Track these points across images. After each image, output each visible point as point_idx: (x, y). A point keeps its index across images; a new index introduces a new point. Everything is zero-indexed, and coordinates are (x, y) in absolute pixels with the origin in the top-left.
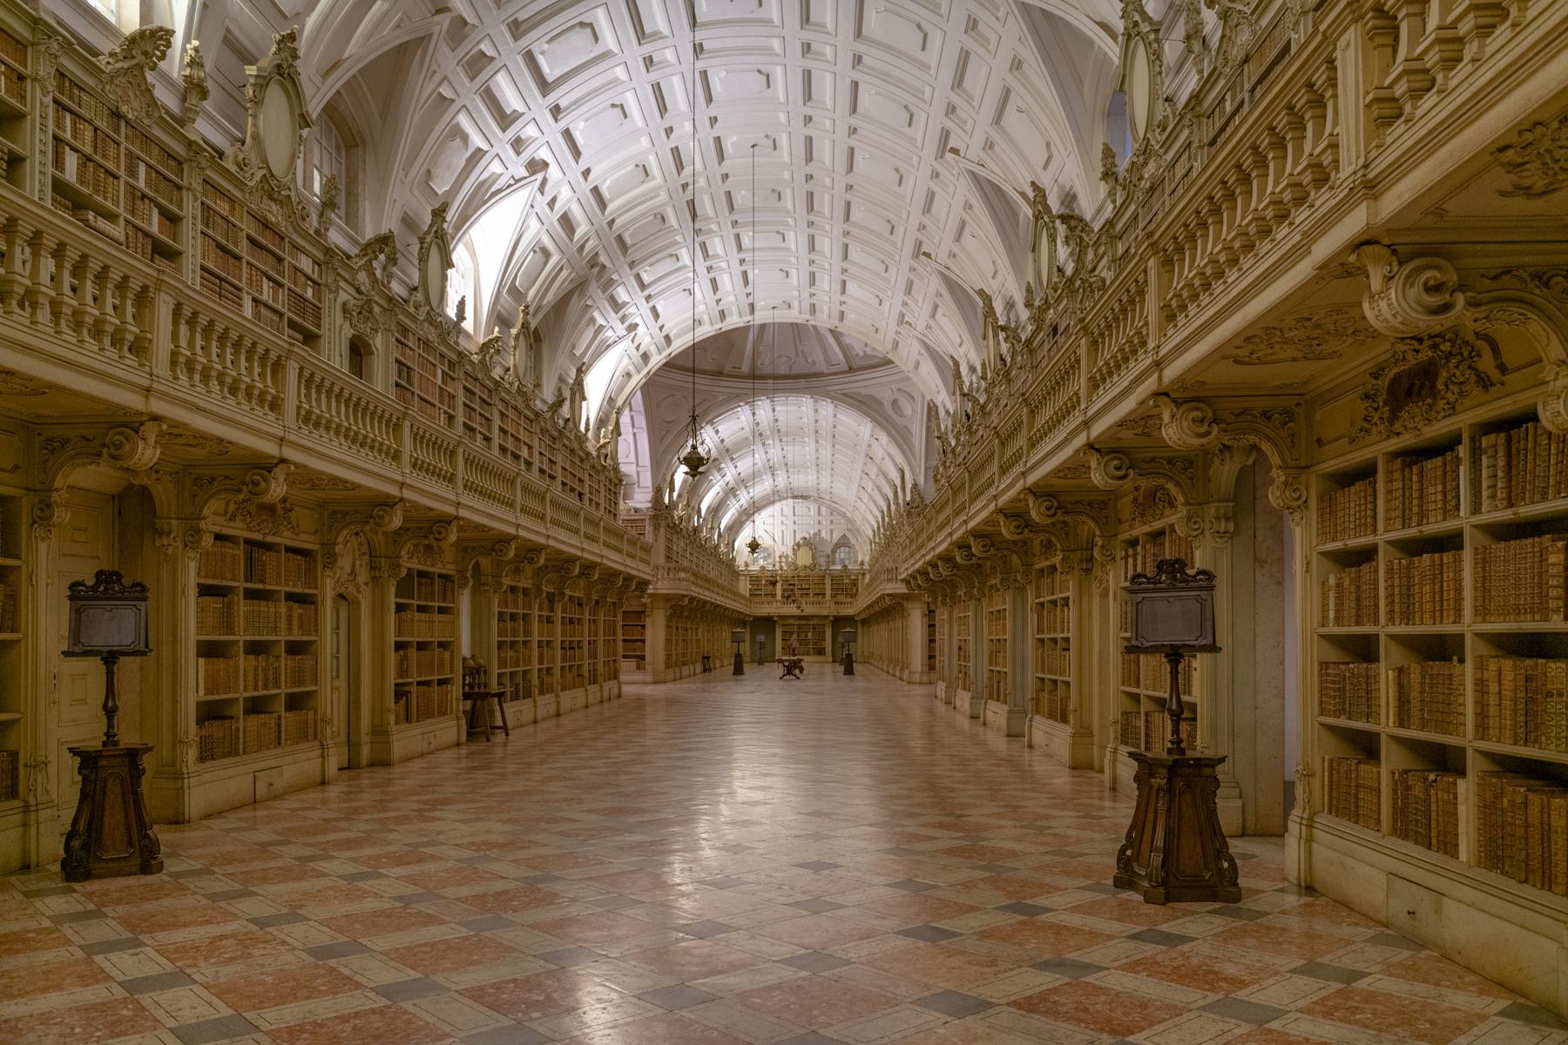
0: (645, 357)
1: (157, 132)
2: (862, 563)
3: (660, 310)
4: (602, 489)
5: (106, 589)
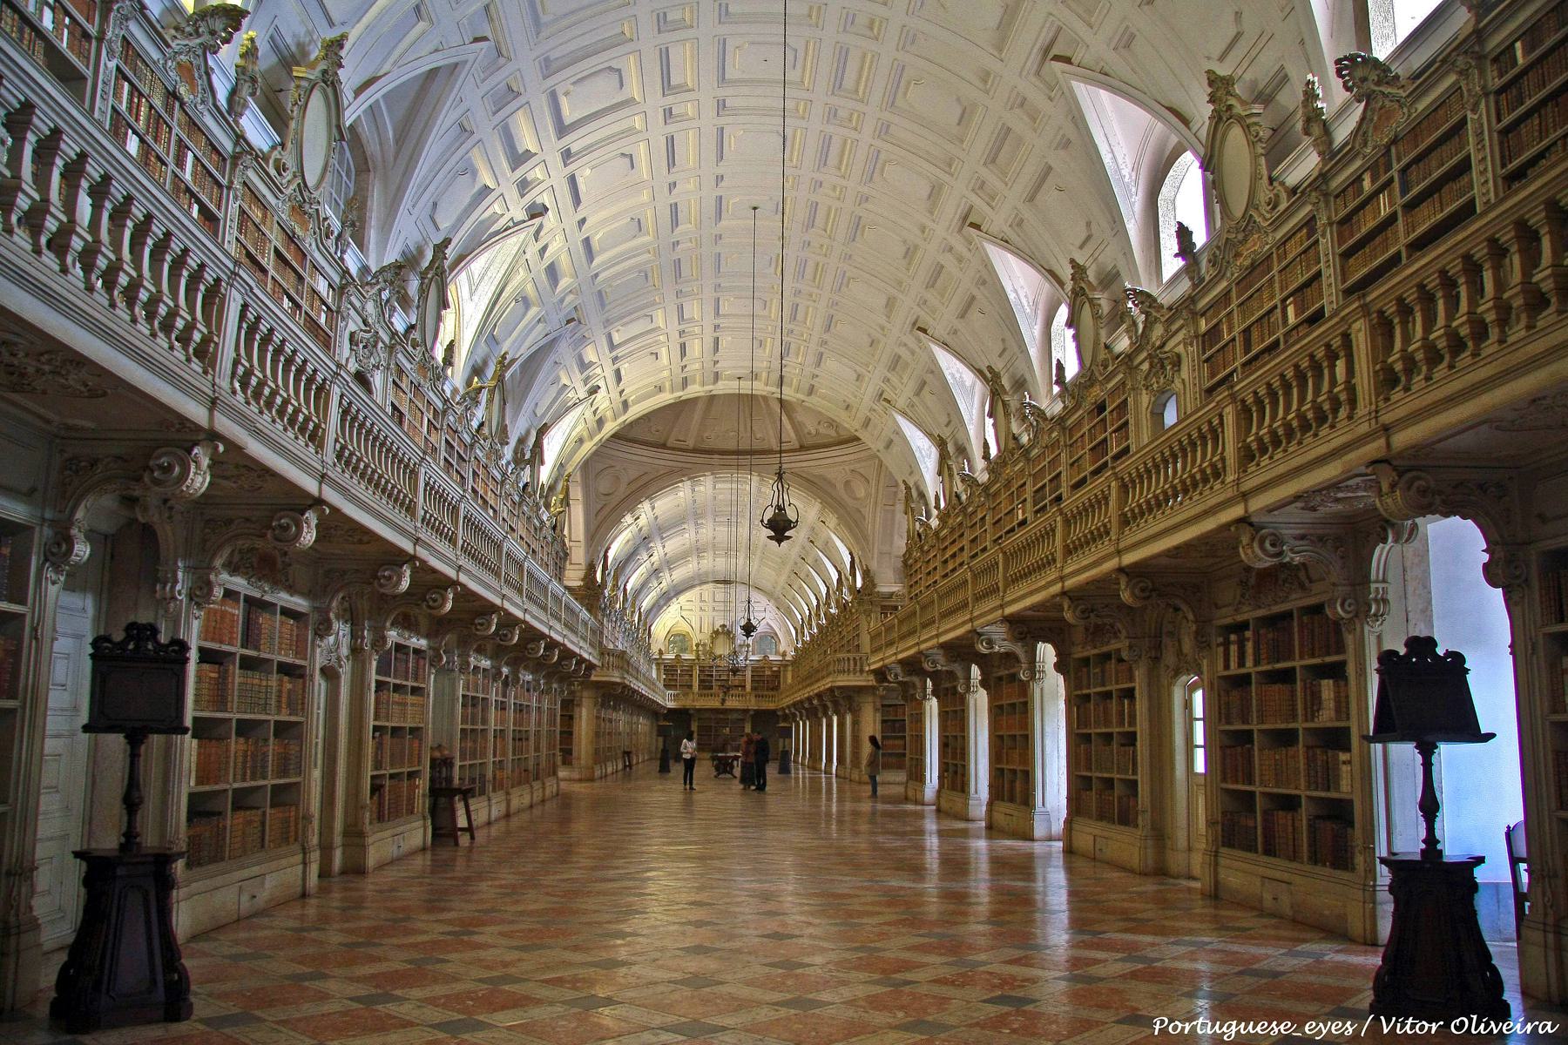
1: (209, 121)
2: (784, 654)
4: (551, 563)
5: (137, 647)
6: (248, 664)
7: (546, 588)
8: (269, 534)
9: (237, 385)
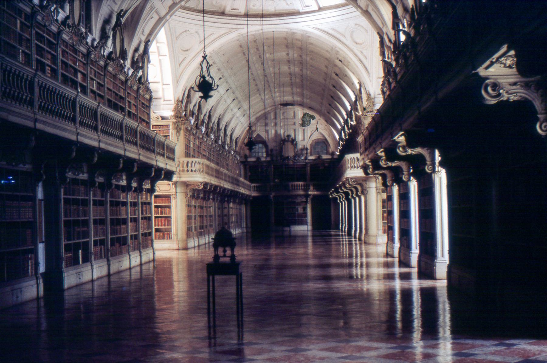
2: (333, 154)
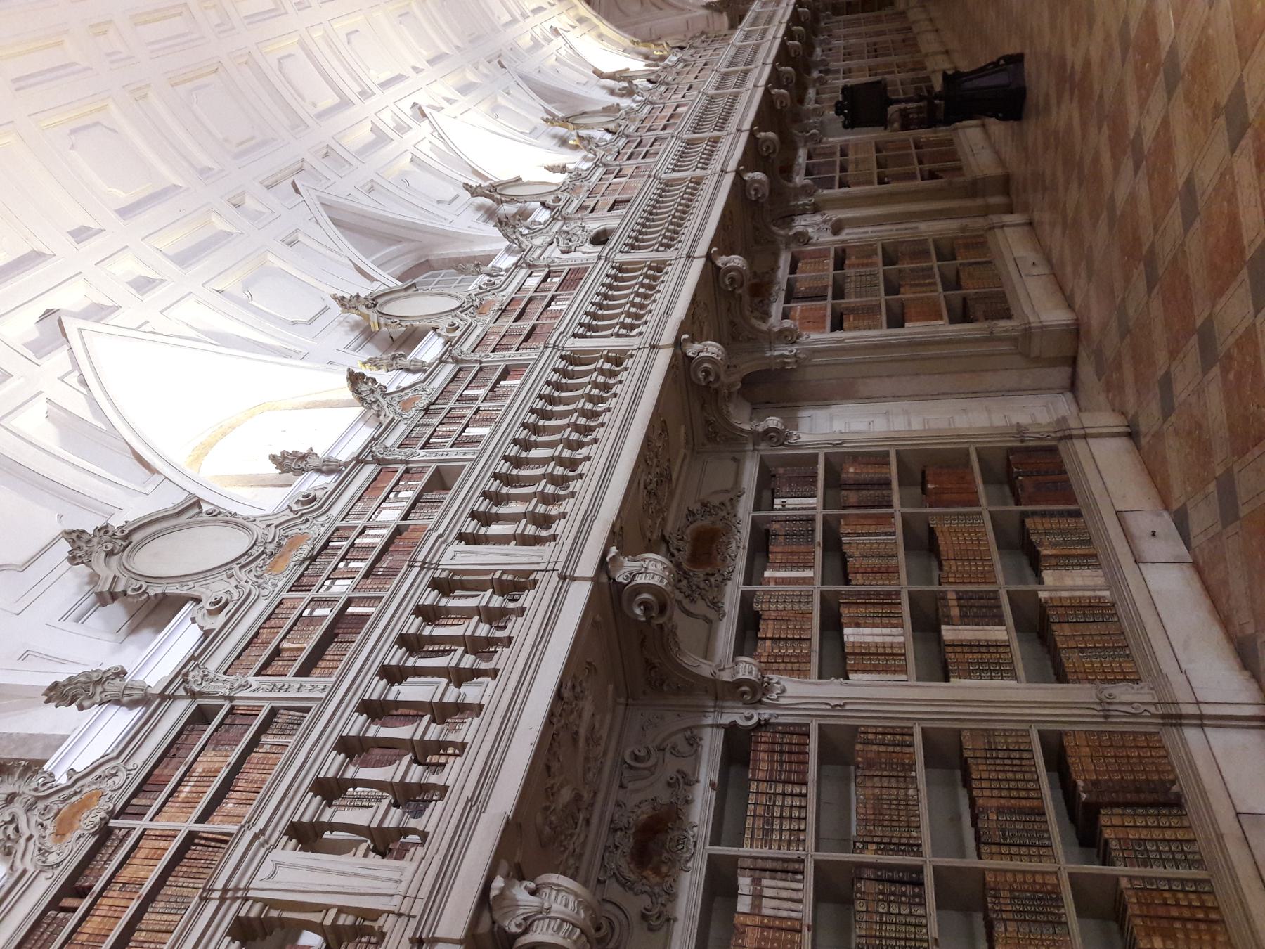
0: (581, 20)
3: (534, 6)
6: (839, 293)
7: (740, 48)
8: (739, 291)
9: (636, 331)
